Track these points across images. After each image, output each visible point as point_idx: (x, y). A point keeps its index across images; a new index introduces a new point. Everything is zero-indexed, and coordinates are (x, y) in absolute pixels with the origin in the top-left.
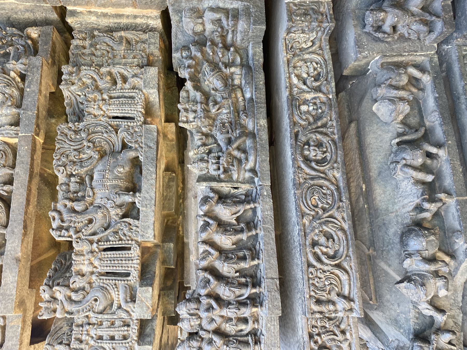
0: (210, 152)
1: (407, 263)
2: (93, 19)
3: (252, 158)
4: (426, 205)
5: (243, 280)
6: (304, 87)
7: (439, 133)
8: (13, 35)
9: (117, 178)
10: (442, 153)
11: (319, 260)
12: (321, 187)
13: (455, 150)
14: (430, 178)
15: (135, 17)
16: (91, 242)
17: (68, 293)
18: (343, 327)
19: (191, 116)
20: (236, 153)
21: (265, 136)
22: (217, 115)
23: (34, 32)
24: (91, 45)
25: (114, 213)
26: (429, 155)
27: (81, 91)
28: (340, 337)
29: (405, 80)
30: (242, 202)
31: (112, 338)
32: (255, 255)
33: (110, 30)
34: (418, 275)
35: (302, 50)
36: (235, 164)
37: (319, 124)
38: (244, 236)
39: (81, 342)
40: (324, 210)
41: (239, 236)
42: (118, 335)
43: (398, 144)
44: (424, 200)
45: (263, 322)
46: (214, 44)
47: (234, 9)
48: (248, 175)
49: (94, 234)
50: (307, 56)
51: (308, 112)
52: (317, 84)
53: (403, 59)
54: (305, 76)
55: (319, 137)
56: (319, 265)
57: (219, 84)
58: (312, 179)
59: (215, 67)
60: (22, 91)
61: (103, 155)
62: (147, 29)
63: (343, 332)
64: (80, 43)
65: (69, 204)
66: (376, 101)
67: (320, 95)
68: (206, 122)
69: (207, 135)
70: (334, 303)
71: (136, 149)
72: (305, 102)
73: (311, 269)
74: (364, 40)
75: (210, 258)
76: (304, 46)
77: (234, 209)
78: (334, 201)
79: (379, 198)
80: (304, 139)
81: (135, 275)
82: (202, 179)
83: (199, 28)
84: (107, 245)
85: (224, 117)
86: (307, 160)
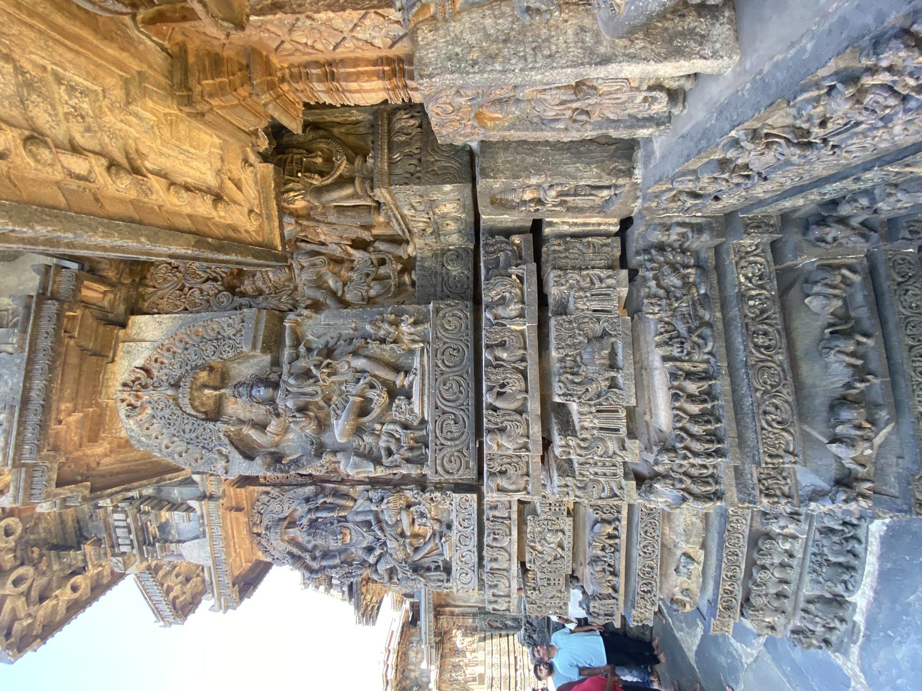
0: (670, 339)
1: (840, 429)
2: (566, 228)
3: (710, 344)
4: (858, 385)
5: (708, 438)
6: (750, 285)
7: (867, 324)
8: (502, 242)
9: (603, 358)
10: (870, 342)
11: (769, 425)
12: (770, 368)
13: (881, 339)
14: (859, 362)
15: (599, 225)
16: (590, 406)
17: (578, 441)
18: (784, 474)
19: (657, 309)
20: (696, 339)
21: (720, 325)
22: (676, 308)
23: (516, 239)
24: (567, 250)
25: (604, 384)
26: (859, 343)
27: (567, 289)
28: (783, 482)
29: (839, 278)
30: (702, 379)
31: (605, 474)
32: (718, 420)
33: (574, 236)
34: (849, 438)
35: (748, 253)
36: (696, 348)
37: (765, 316)
38: (709, 406)
39: (583, 476)
40: (772, 386)
41: (705, 405)
42: (608, 472)
43: (831, 333)
44: (855, 380)
45: (722, 468)
46: (674, 249)
47: (697, 224)
48: (706, 357)
49: (590, 400)
50: (751, 259)
51: (754, 306)
52: (760, 282)
53: (837, 261)
54: (750, 275)
55: (766, 327)
56: (770, 429)
57: (678, 283)
58: (762, 361)
59: (674, 268)
60: (522, 290)
61: (589, 341)
62: (608, 235)
63: (785, 478)
64: (557, 248)
65: (570, 377)
66: (808, 296)
67: (763, 292)
68: (670, 313)
69: (668, 323)
70: (781, 457)
71: (615, 336)
72: (752, 298)
73: (764, 432)
74: (805, 245)
75: (685, 421)
76: (749, 249)
77: (700, 384)
78: (780, 379)
79: (805, 374)
80: (753, 329)
81: (623, 431)
82: (665, 359)
83: (665, 239)
84: (602, 408)
85: (684, 309)
86: (757, 346)
